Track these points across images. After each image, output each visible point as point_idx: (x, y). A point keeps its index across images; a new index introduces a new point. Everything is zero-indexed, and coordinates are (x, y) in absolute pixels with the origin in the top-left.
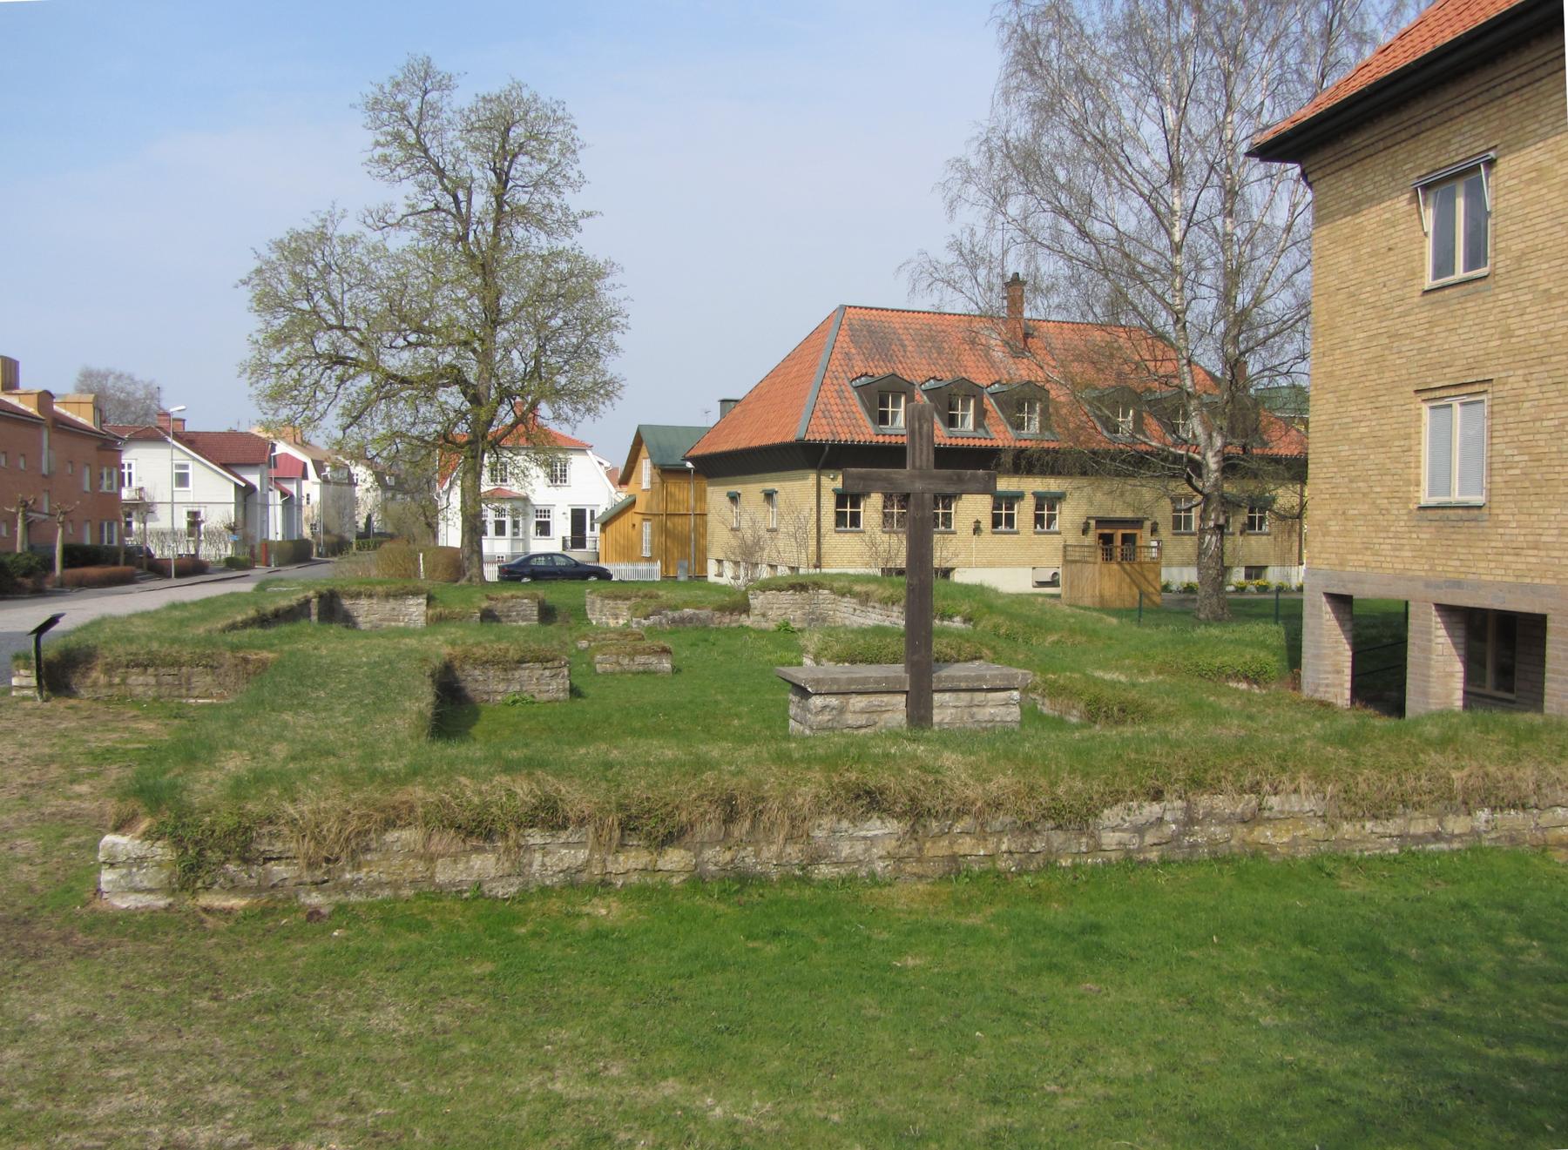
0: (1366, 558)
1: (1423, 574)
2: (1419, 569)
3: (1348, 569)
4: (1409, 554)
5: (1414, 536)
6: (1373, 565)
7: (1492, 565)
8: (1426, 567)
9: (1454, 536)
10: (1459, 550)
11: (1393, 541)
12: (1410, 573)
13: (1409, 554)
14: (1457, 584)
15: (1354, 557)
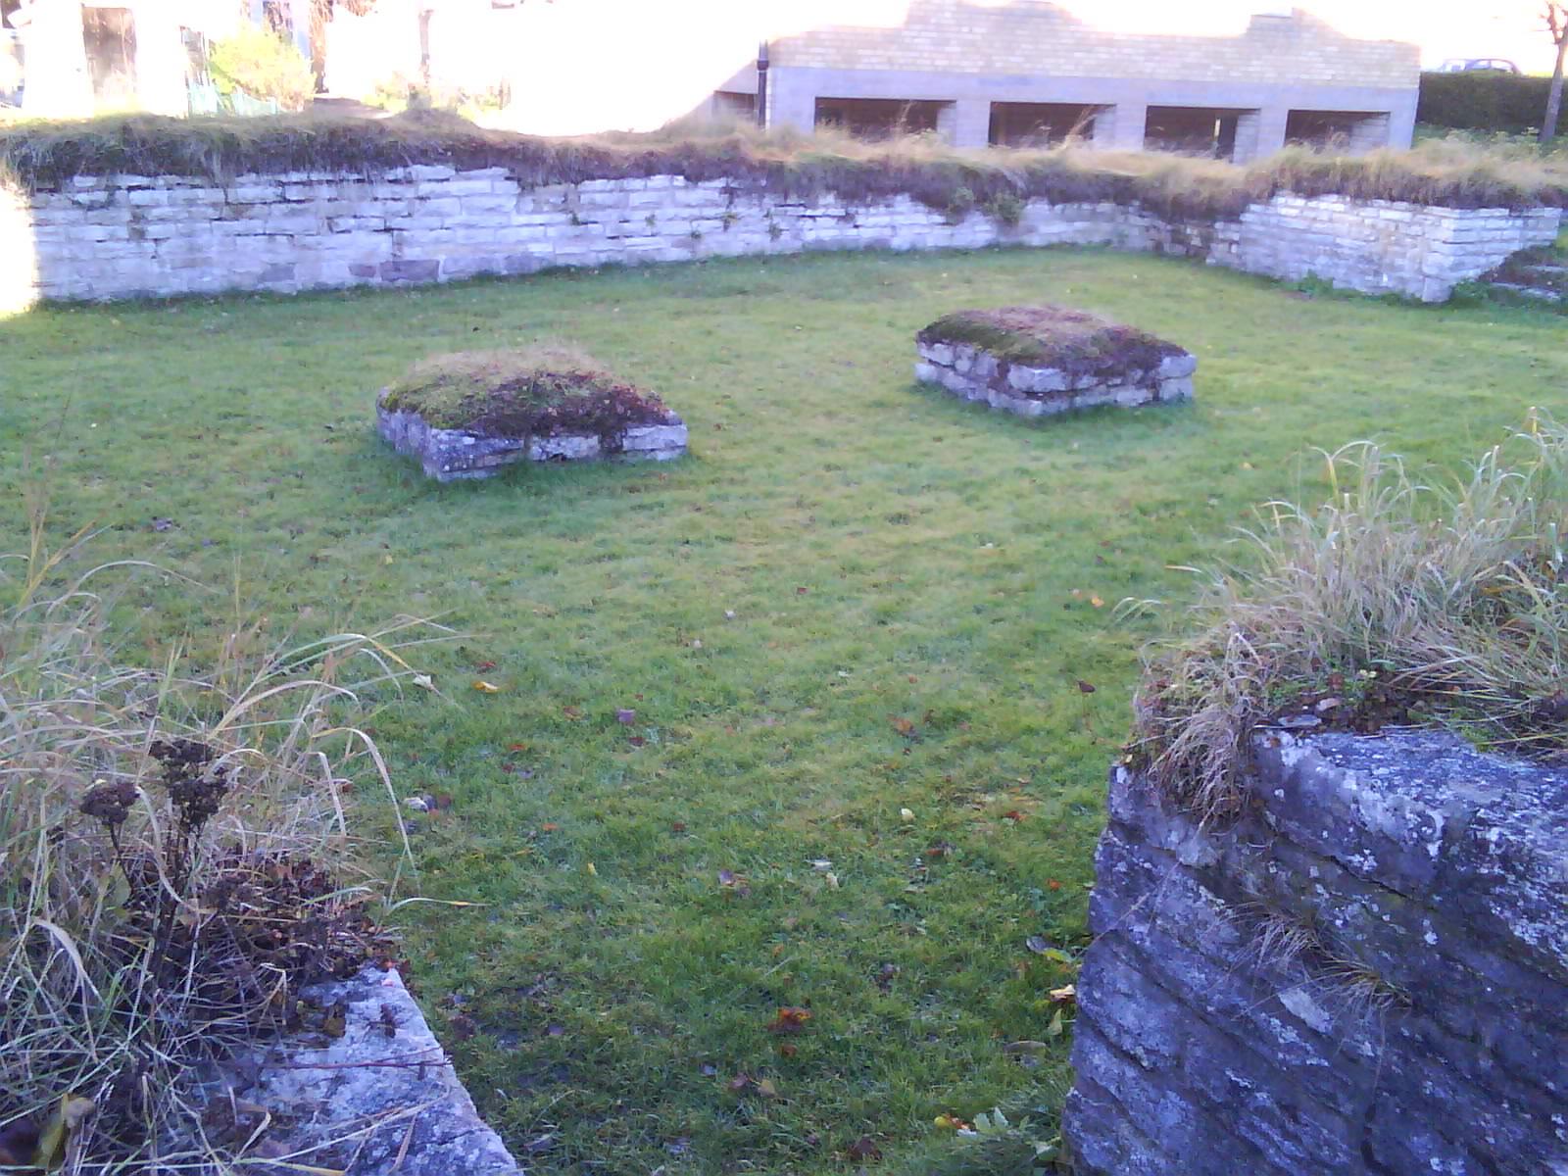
0: (890, 53)
1: (976, 70)
2: (972, 66)
3: (859, 67)
4: (957, 49)
5: (965, 29)
6: (902, 61)
7: (1062, 61)
8: (981, 63)
9: (1019, 32)
10: (1024, 46)
11: (934, 35)
12: (958, 70)
13: (957, 49)
14: (1024, 81)
15: (869, 52)
